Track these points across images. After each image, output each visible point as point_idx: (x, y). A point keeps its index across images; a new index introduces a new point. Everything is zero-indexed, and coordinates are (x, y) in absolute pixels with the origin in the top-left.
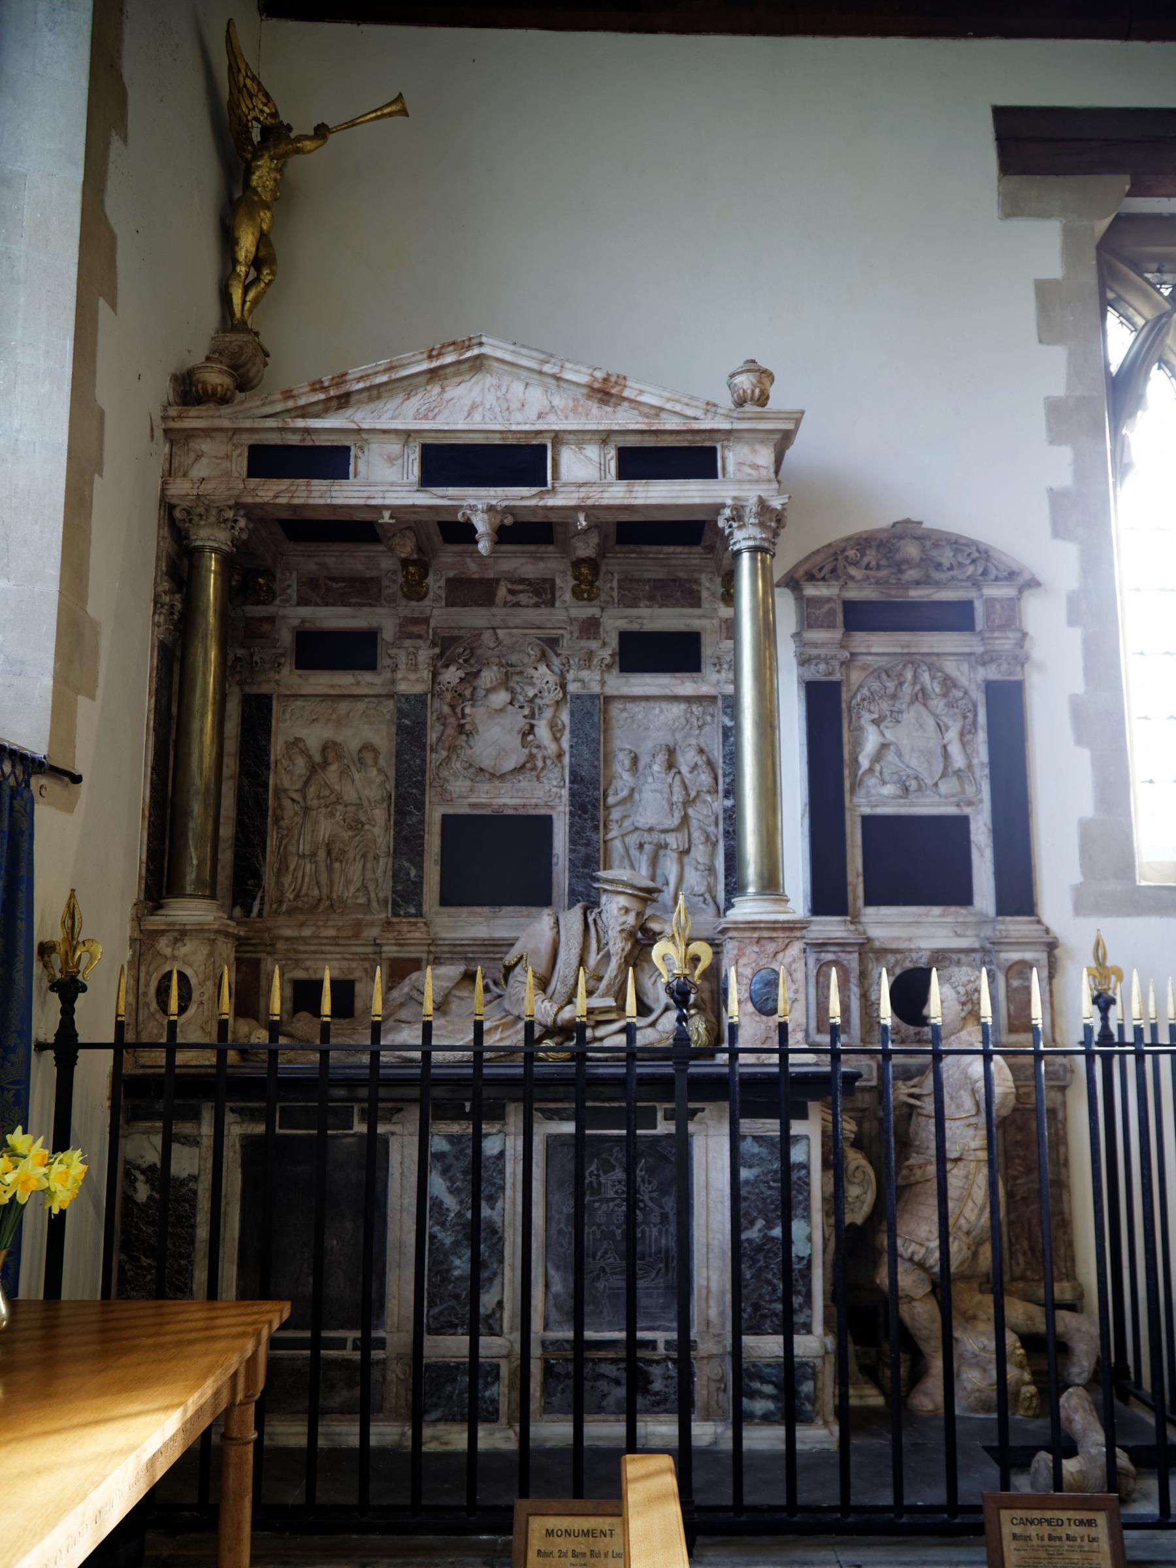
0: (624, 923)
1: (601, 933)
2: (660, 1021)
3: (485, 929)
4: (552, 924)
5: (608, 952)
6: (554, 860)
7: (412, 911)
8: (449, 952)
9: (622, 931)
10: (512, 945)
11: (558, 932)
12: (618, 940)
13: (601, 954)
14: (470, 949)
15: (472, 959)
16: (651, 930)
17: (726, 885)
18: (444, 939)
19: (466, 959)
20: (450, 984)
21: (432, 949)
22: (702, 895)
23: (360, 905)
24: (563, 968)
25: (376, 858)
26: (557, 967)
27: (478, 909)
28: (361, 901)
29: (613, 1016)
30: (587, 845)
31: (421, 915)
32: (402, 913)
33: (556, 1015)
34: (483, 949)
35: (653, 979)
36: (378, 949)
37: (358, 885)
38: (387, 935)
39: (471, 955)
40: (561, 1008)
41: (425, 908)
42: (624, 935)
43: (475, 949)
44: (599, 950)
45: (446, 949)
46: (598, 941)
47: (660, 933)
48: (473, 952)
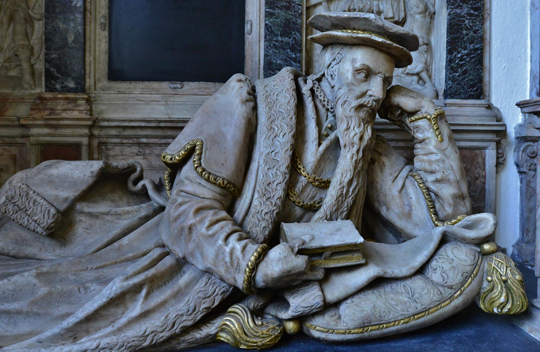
0: (363, 95)
1: (322, 111)
2: (434, 263)
3: (162, 108)
4: (244, 94)
5: (336, 143)
6: (247, 27)
7: (72, 85)
8: (117, 136)
9: (360, 107)
10: (182, 128)
11: (255, 108)
12: (354, 123)
13: (325, 144)
14: (144, 132)
15: (146, 145)
16: (398, 107)
17: (449, 62)
18: (108, 120)
19: (139, 144)
20: (71, 194)
21: (96, 132)
22: (418, 74)
23: (11, 77)
24: (263, 168)
25: (29, 20)
26: (254, 166)
27: (155, 85)
28: (12, 73)
29: (356, 259)
30: (288, 8)
31: (83, 90)
32: (58, 86)
33: (255, 268)
34: (159, 133)
35: (399, 182)
36: (25, 132)
37: (8, 54)
38: (38, 115)
39: (144, 140)
40: (262, 256)
41: (89, 82)
42: (362, 114)
43: (149, 132)
44: (321, 138)
45: (113, 132)
46: (319, 124)
47: (412, 113)
48: (147, 137)
